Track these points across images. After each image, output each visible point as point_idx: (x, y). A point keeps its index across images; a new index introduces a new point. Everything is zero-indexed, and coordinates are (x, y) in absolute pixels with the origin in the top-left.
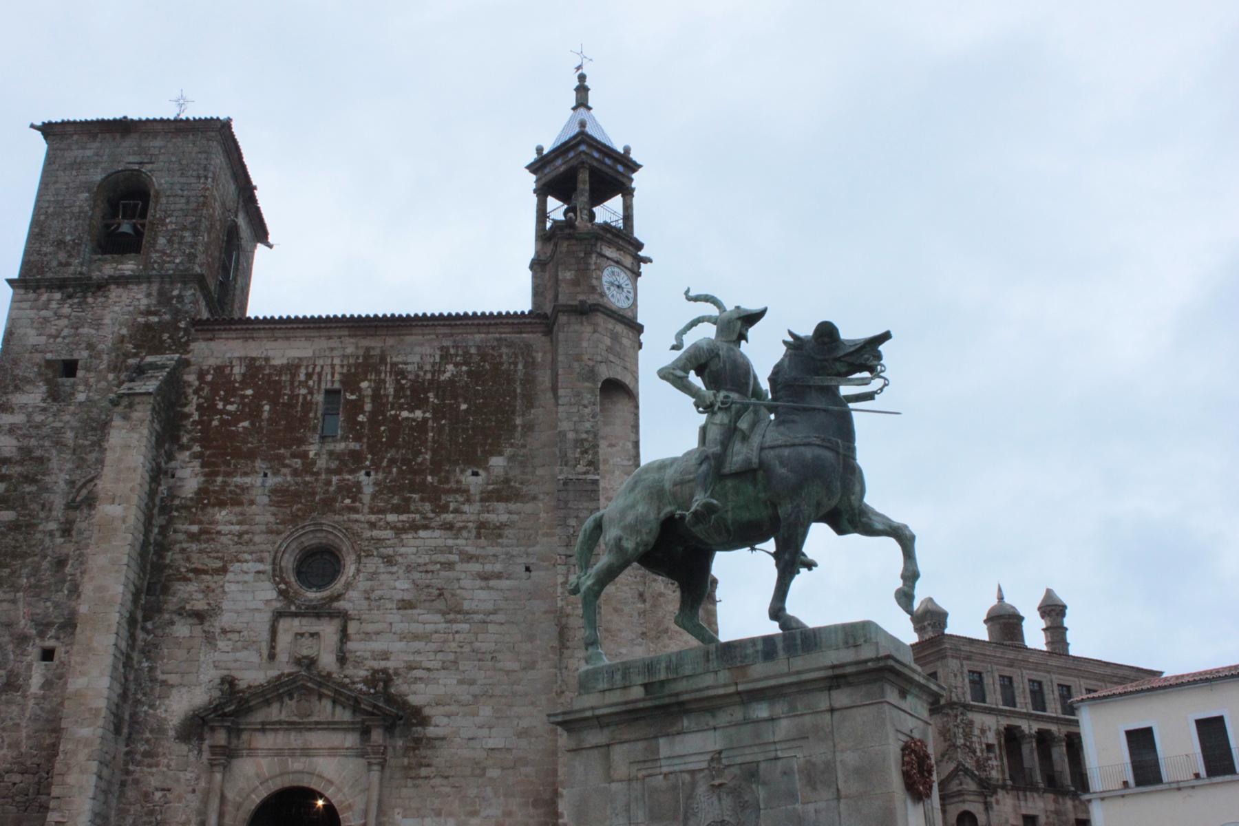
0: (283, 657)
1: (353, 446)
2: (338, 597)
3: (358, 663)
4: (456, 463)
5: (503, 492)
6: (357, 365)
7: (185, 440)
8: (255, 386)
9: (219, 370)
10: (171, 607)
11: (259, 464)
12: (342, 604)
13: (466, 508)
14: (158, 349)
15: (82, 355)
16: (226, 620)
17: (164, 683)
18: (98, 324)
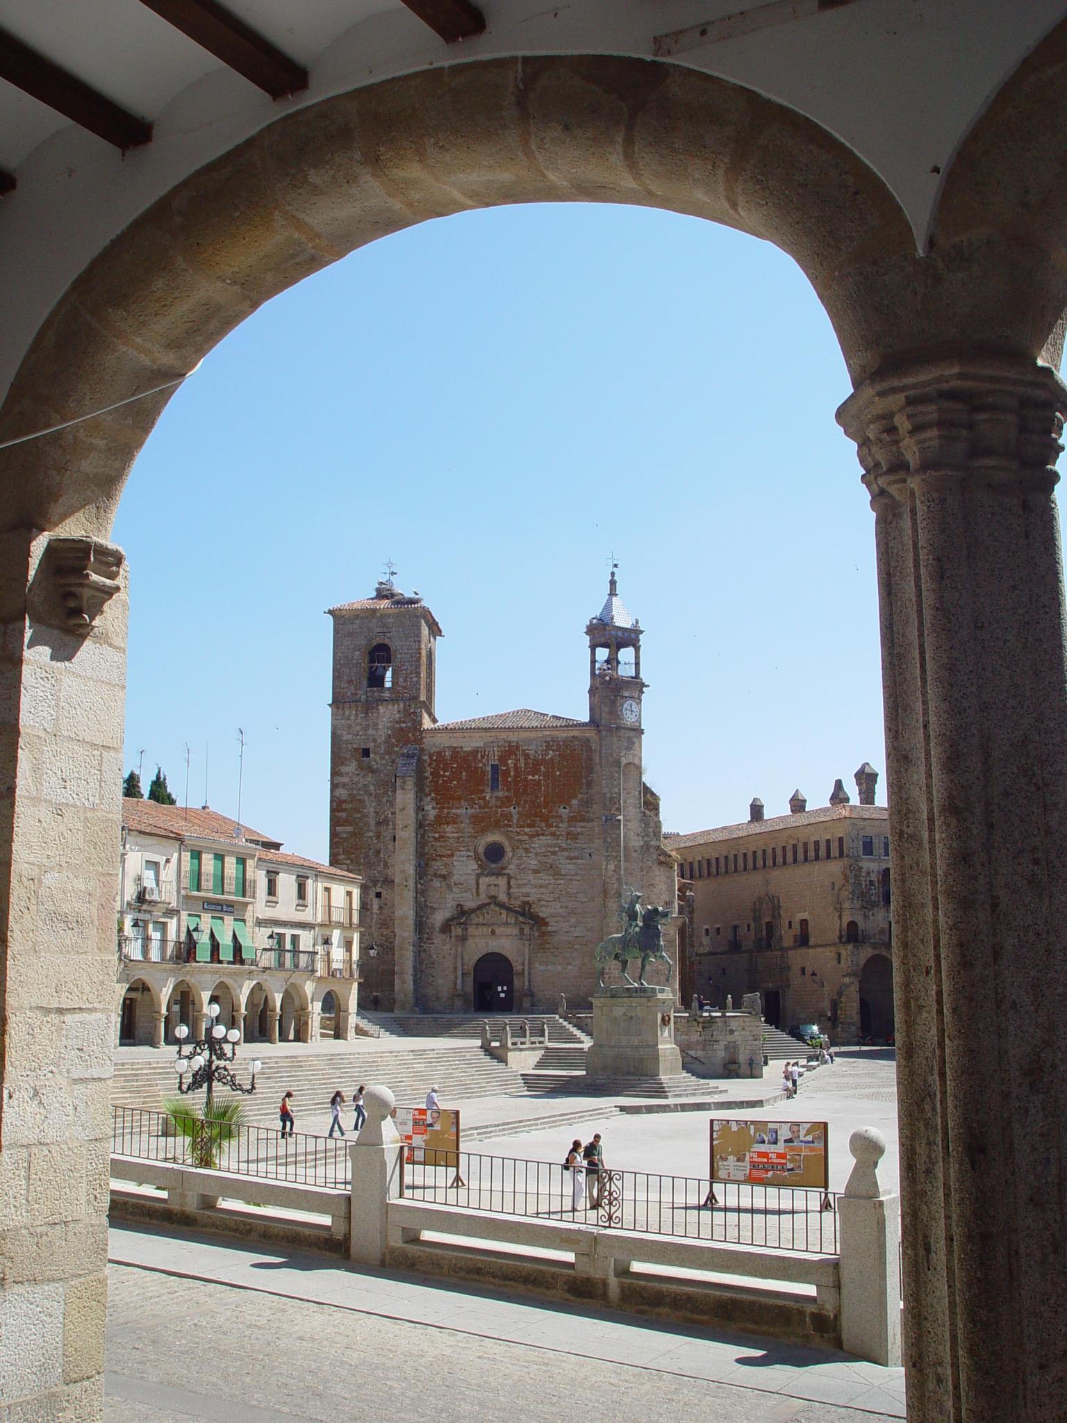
0: (483, 896)
2: (505, 868)
3: (516, 899)
5: (578, 818)
7: (427, 790)
9: (439, 753)
14: (407, 742)
15: (371, 745)
16: (455, 878)
18: (377, 729)
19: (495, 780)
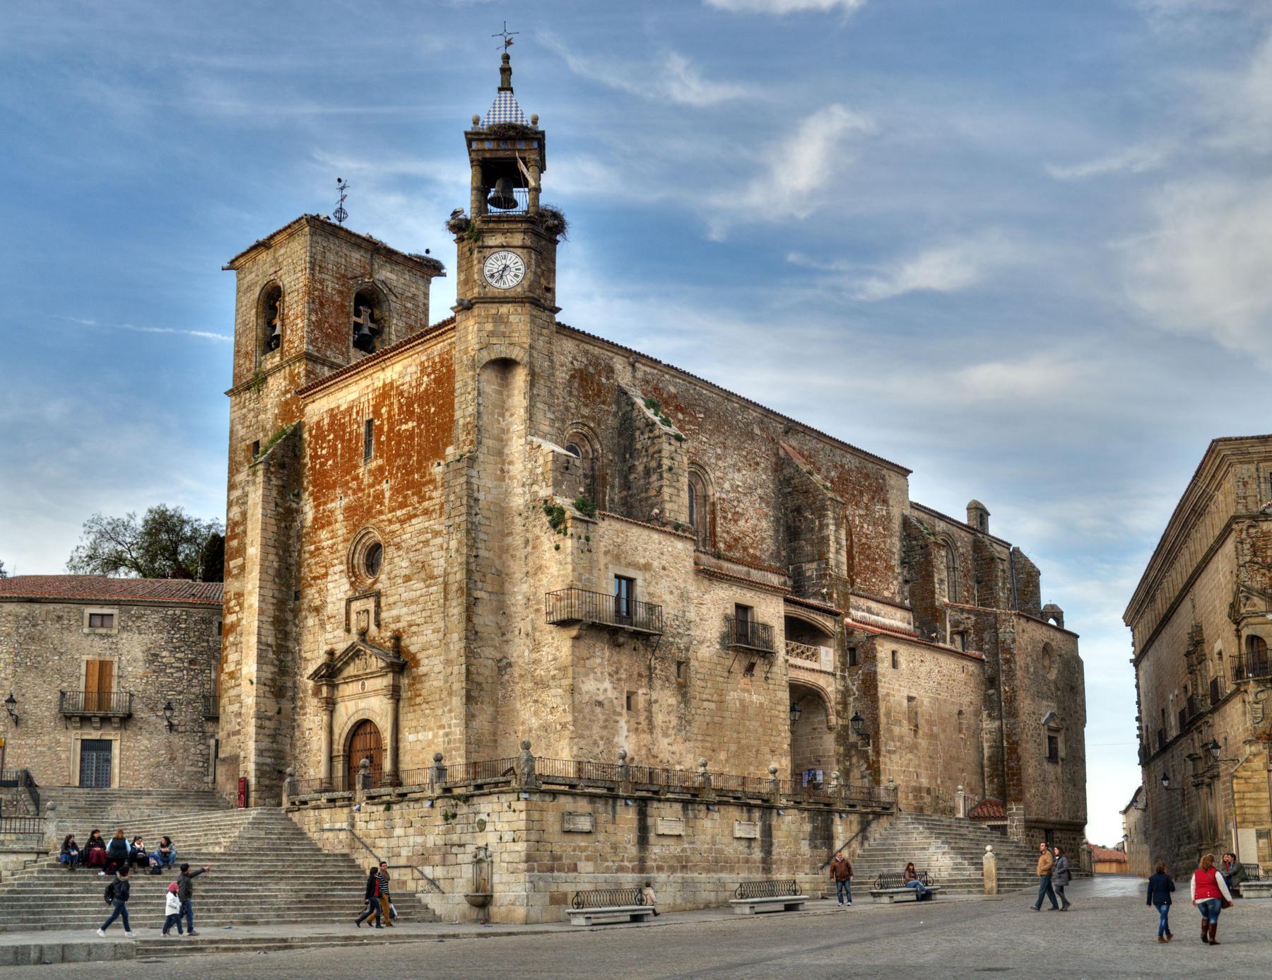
0: (354, 630)
1: (380, 462)
4: (429, 459)
6: (380, 395)
8: (335, 432)
9: (318, 423)
10: (305, 606)
11: (339, 491)
12: (378, 586)
13: (434, 494)
16: (330, 609)
17: (306, 659)
19: (368, 444)
